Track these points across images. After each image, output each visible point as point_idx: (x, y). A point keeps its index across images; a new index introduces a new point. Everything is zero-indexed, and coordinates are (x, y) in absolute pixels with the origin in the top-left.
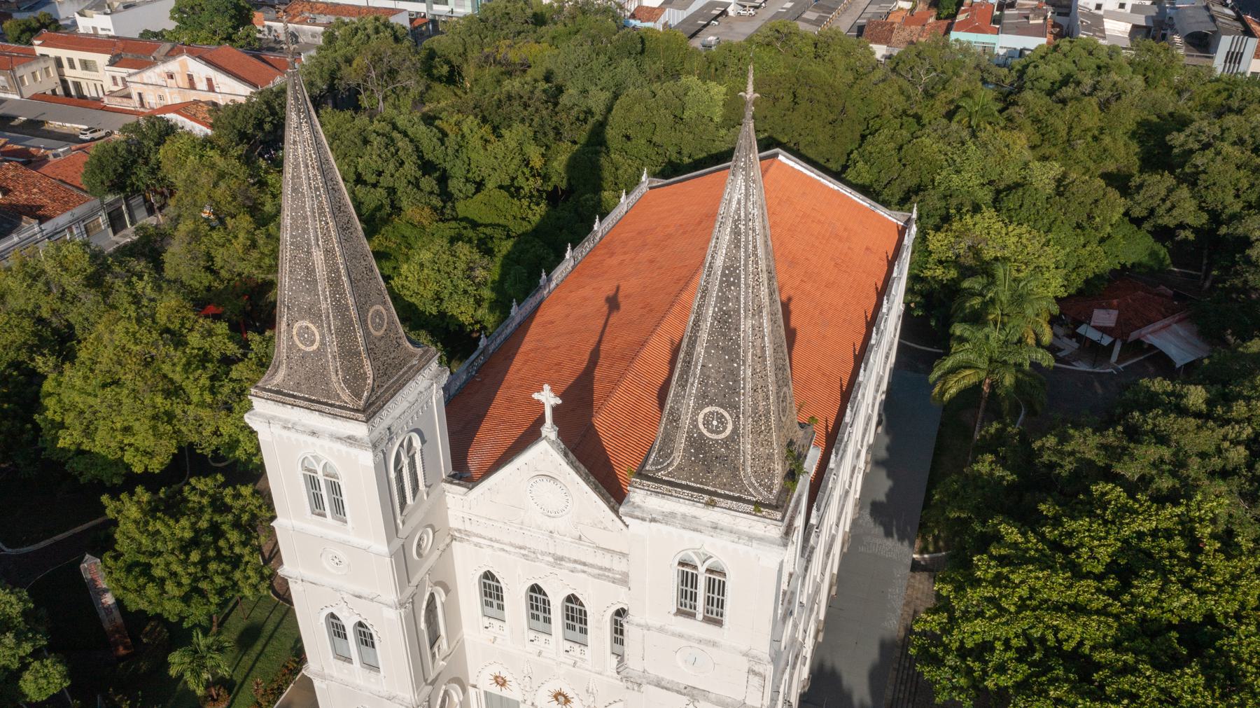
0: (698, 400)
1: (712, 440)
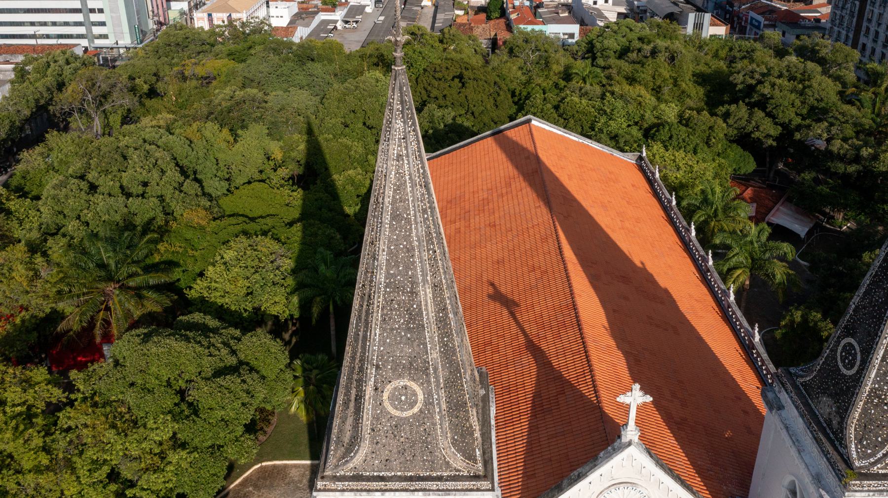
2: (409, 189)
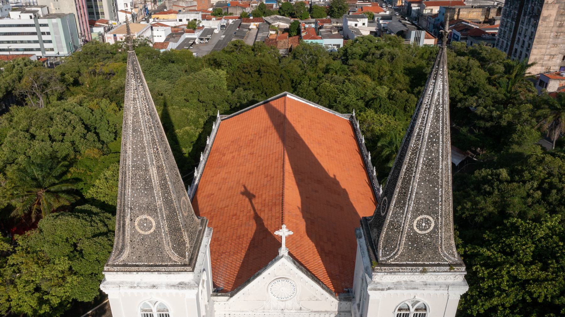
2: (141, 116)
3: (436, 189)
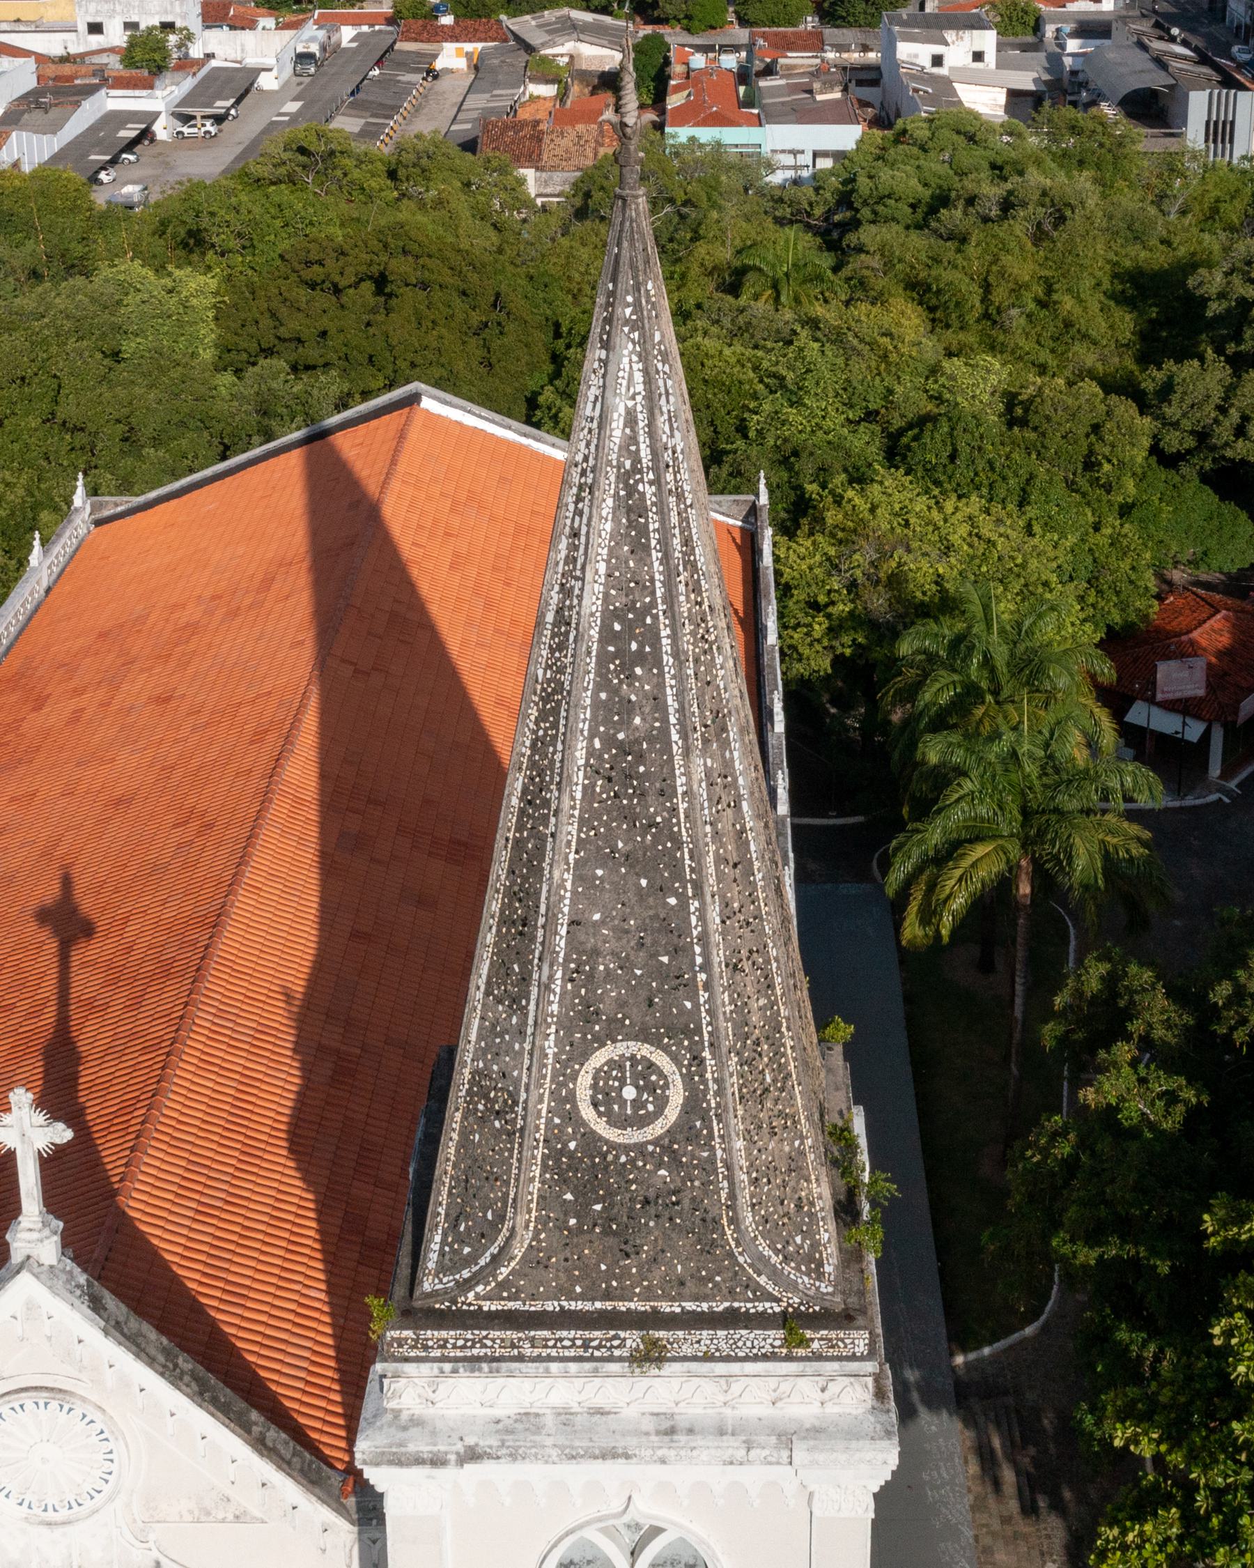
0: (570, 1032)
1: (626, 1148)
3: (672, 901)
